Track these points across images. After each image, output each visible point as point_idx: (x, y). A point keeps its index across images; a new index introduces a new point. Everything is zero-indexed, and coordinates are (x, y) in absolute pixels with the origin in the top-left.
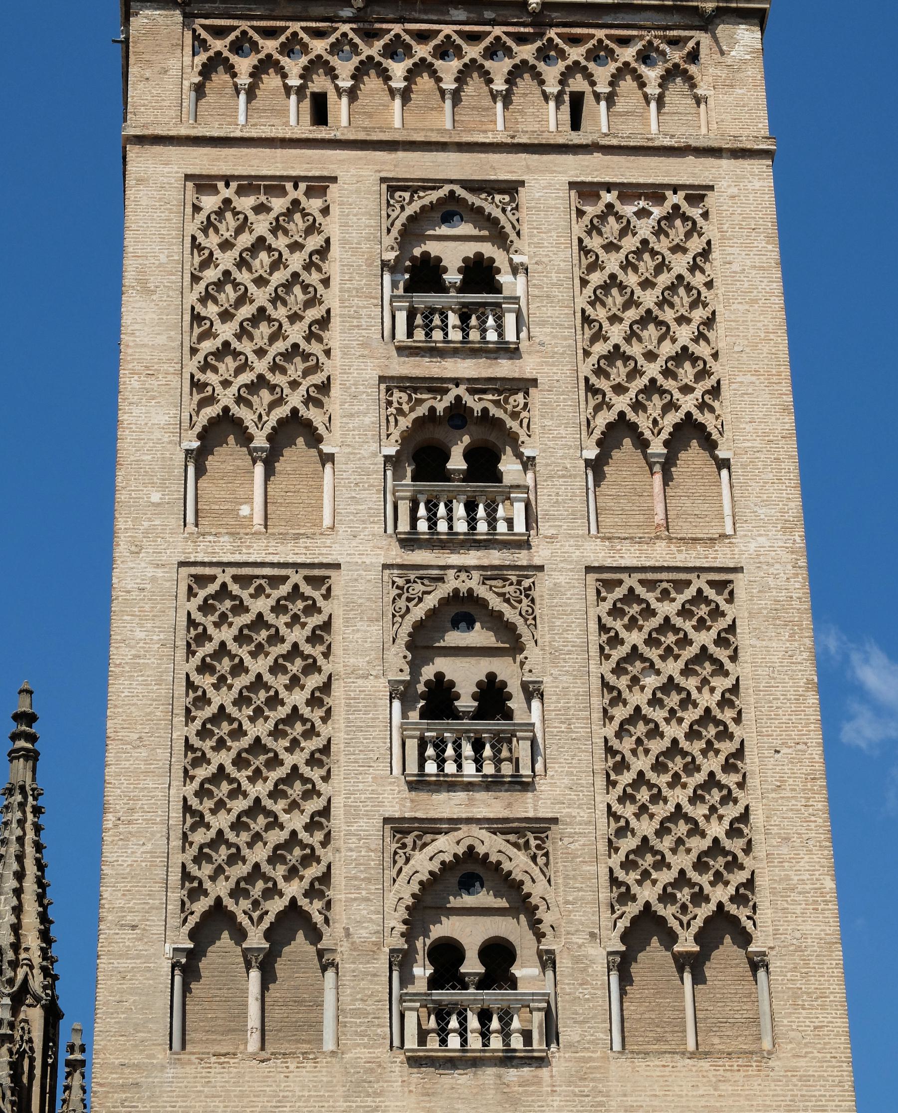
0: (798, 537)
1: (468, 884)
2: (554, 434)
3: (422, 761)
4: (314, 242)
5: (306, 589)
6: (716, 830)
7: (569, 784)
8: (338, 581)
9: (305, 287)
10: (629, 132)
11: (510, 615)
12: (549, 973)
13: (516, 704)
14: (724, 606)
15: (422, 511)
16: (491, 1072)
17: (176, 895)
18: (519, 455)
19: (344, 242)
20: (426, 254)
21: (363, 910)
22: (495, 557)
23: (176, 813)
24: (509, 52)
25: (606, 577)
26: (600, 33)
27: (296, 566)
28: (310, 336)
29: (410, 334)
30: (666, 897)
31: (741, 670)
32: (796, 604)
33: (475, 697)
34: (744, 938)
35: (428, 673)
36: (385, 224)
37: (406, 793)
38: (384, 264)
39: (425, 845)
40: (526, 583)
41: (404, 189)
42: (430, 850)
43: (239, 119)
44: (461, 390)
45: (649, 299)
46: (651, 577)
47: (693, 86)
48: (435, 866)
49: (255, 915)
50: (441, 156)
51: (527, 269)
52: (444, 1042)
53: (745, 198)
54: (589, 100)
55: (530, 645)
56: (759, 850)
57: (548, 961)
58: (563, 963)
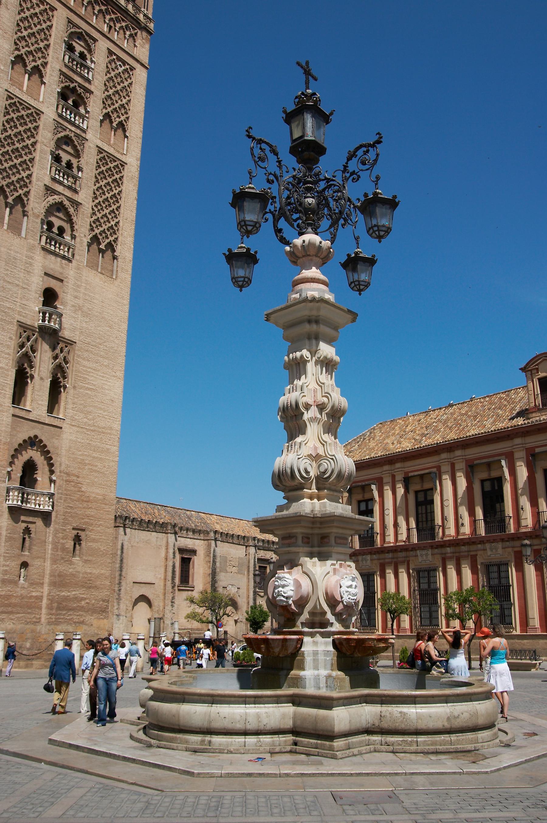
0: (139, 162)
1: (59, 210)
4: (48, 23)
5: (34, 114)
7: (85, 196)
8: (43, 117)
9: (45, 34)
11: (79, 147)
12: (73, 240)
13: (75, 170)
16: (59, 259)
18: (86, 109)
19: (56, 28)
20: (72, 44)
21: (37, 205)
22: (78, 131)
24: (99, 5)
25: (100, 151)
26: (119, 15)
27: (35, 108)
28: (44, 48)
31: (124, 188)
33: (66, 164)
34: (114, 251)
35: (57, 152)
37: (50, 180)
38: (65, 40)
39: (52, 196)
40: (83, 142)
41: (72, 24)
44: (76, 84)
45: (119, 88)
46: (109, 155)
47: (135, 42)
50: (82, 21)
54: (113, 30)
56: (120, 232)
57: (73, 237)
58: (78, 239)
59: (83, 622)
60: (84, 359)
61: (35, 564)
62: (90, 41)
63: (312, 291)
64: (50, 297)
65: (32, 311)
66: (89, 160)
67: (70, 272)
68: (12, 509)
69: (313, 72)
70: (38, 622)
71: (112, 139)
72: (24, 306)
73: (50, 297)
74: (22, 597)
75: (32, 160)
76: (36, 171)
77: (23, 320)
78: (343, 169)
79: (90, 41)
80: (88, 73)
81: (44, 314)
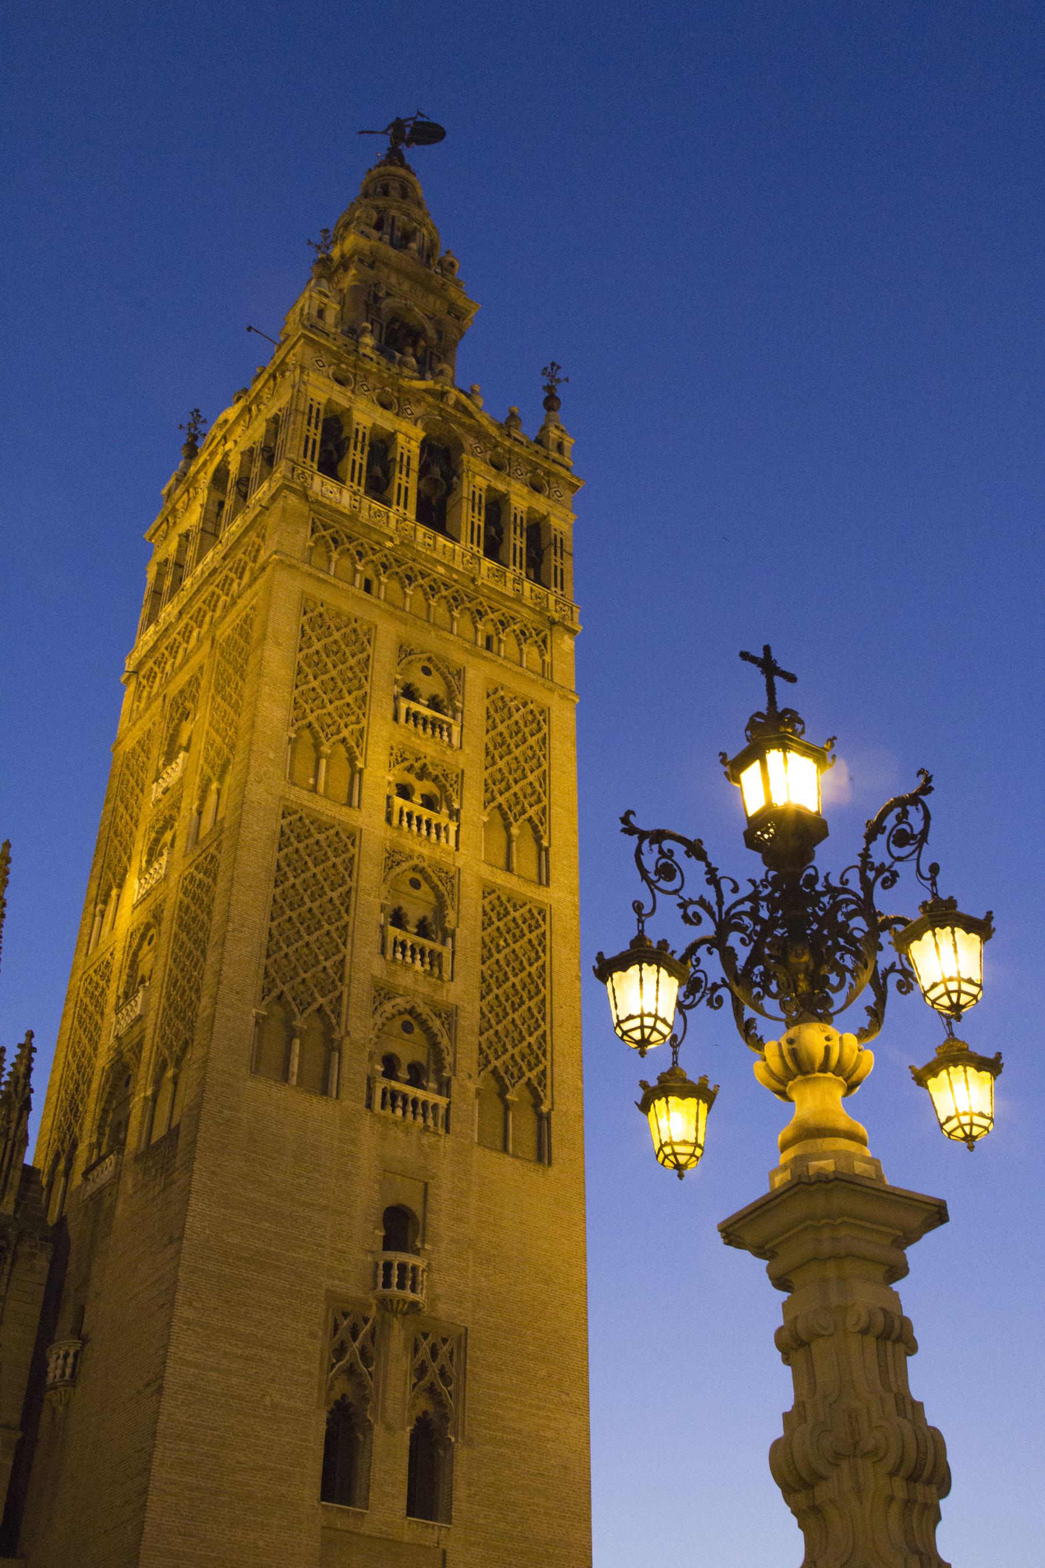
3: (394, 952)
7: (462, 990)
11: (441, 888)
14: (541, 922)
15: (405, 819)
17: (261, 982)
22: (438, 855)
23: (265, 937)
26: (504, 610)
29: (407, 721)
32: (574, 933)
33: (417, 927)
36: (398, 660)
42: (393, 1002)
48: (395, 1011)
49: (301, 1008)
51: (462, 713)
52: (393, 1111)
54: (495, 639)
55: (450, 908)
63: (820, 1159)
64: (400, 1226)
69: (782, 664)
71: (515, 860)
78: (859, 864)
80: (450, 736)
81: (388, 1266)
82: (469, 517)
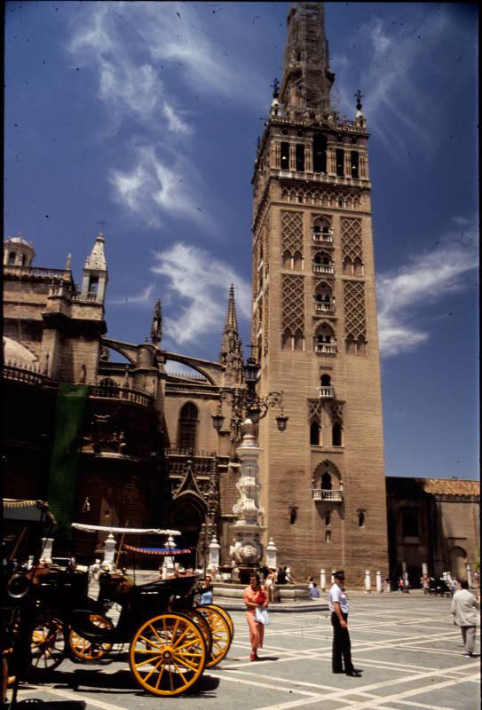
2: (337, 257)
6: (361, 322)
7: (340, 314)
10: (348, 209)
25: (345, 281)
30: (353, 331)
31: (366, 297)
43: (288, 201)
45: (352, 237)
53: (367, 221)
59: (370, 565)
60: (354, 409)
61: (335, 532)
62: (328, 219)
64: (325, 380)
65: (318, 392)
66: (338, 291)
67: (336, 362)
68: (317, 502)
70: (341, 564)
72: (309, 389)
73: (325, 380)
74: (329, 550)
75: (302, 306)
76: (306, 311)
77: (312, 397)
79: (328, 219)
82: (331, 163)
